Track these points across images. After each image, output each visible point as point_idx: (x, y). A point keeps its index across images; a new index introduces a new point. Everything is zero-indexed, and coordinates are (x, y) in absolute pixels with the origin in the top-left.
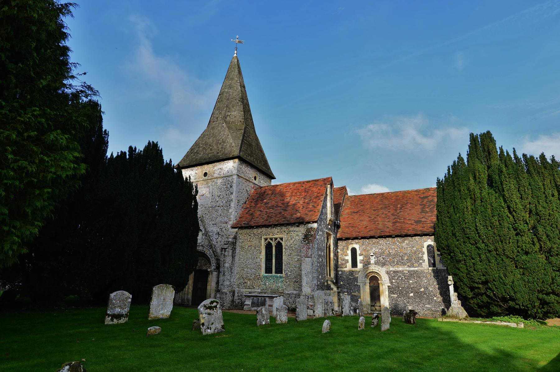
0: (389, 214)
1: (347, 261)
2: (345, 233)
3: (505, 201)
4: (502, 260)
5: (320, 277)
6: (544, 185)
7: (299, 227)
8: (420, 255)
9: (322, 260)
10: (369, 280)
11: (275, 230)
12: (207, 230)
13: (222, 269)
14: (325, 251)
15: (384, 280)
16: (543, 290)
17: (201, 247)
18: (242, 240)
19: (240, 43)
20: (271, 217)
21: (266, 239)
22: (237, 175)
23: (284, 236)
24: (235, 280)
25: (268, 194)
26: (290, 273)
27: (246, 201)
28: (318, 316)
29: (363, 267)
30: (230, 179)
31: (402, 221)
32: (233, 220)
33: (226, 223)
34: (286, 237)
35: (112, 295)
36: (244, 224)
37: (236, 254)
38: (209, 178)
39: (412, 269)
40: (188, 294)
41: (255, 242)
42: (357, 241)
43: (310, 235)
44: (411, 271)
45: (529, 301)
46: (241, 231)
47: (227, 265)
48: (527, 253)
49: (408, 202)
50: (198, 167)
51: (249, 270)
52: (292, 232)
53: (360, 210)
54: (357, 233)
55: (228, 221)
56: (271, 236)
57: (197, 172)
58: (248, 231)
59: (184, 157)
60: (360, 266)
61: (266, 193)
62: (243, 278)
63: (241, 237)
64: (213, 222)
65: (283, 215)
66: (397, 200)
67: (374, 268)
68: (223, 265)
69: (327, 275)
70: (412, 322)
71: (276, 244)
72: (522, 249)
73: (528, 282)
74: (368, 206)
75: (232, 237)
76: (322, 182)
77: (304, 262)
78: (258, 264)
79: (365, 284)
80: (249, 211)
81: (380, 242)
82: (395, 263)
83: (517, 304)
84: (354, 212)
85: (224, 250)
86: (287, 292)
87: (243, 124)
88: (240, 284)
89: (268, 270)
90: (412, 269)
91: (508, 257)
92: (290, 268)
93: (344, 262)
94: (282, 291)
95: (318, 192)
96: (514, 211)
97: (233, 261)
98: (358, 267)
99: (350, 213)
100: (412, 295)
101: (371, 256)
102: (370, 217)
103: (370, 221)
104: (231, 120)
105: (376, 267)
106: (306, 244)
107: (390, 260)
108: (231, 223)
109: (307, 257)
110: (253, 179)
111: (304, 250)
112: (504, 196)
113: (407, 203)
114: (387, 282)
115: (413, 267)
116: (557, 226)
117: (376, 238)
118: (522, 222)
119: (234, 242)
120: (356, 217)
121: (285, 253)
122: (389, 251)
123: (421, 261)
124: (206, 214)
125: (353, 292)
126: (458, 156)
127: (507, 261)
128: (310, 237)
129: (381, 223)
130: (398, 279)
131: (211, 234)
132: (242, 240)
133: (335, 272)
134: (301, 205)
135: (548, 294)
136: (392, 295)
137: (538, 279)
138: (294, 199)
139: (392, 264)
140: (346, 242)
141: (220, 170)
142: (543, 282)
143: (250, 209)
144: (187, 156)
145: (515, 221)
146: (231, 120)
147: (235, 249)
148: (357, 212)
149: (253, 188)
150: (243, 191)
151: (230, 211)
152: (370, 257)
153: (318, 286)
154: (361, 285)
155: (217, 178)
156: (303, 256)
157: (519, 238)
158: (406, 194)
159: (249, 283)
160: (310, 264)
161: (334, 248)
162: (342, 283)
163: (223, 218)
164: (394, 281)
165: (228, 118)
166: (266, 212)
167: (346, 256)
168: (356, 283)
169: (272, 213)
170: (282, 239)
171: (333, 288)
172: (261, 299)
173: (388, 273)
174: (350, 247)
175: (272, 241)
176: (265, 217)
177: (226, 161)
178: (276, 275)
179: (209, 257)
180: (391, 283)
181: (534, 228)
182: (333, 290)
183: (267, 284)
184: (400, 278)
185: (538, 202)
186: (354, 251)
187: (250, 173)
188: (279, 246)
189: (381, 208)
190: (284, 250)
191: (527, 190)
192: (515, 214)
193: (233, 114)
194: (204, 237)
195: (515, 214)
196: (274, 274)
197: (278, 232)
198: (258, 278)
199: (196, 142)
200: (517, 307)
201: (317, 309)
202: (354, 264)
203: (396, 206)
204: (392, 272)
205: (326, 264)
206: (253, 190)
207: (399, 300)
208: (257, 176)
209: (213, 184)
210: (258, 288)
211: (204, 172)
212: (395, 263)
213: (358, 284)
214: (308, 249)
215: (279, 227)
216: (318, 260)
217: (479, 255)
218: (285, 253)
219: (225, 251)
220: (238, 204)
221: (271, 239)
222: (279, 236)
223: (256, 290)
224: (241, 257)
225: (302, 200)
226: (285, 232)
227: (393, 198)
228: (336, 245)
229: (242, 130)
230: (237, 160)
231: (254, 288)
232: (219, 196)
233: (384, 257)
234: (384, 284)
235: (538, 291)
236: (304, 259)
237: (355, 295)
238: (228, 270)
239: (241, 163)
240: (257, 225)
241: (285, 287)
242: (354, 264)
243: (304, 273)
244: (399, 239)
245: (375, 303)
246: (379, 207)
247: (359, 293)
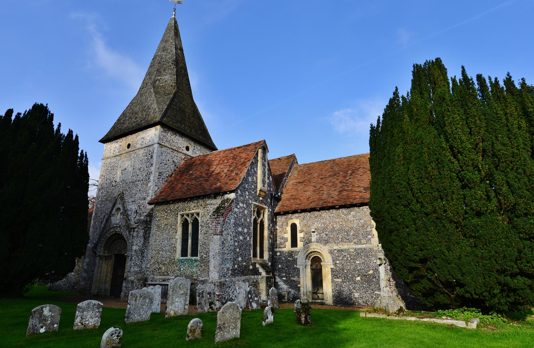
0: (337, 182)
1: (286, 240)
2: (284, 206)
3: (447, 140)
4: (444, 226)
5: (240, 259)
6: (506, 114)
7: (216, 199)
8: (369, 229)
9: (245, 239)
10: (311, 262)
11: (192, 204)
12: (126, 209)
13: (130, 253)
14: (252, 228)
15: (326, 261)
16: (506, 270)
17: (118, 228)
18: (159, 218)
20: (190, 190)
21: (182, 216)
22: (158, 143)
23: (200, 211)
24: (148, 266)
25: (196, 165)
26: (205, 256)
27: (172, 174)
28: (175, 313)
29: (304, 246)
30: (151, 149)
31: (350, 188)
32: (151, 195)
33: (145, 199)
37: (151, 235)
39: (359, 246)
40: (105, 283)
41: (171, 220)
42: (297, 215)
43: (222, 207)
44: (359, 249)
45: (486, 287)
46: (158, 208)
48: (479, 214)
49: (361, 166)
50: (122, 138)
51: (164, 253)
52: (209, 206)
53: (306, 180)
54: (297, 206)
55: (146, 196)
56: (187, 212)
57: (121, 144)
58: (165, 207)
59: (111, 129)
60: (300, 244)
61: (194, 164)
62: (158, 262)
63: (157, 215)
64: (133, 199)
66: (348, 165)
67: (315, 247)
68: (131, 248)
69: (255, 255)
70: (303, 322)
71: (193, 220)
72: (471, 209)
73: (483, 258)
74: (316, 175)
75: (145, 214)
76: (254, 146)
77: (212, 241)
78: (173, 246)
79: (306, 267)
80: (172, 184)
81: (323, 215)
82: (340, 240)
83: (467, 292)
84: (299, 183)
85: (132, 230)
86: (201, 279)
87: (174, 89)
88: (155, 269)
89: (184, 253)
90: (359, 246)
91: (451, 221)
92: (206, 249)
93: (283, 241)
94: (196, 278)
95: (246, 157)
96: (459, 152)
97: (144, 244)
98: (298, 246)
99: (295, 184)
100: (358, 278)
101: (313, 232)
102: (315, 187)
103: (314, 191)
104: (161, 85)
105: (318, 246)
106: (216, 218)
107: (334, 236)
108: (149, 199)
109: (216, 235)
110: (184, 149)
111: (213, 226)
112: (445, 133)
113: (359, 168)
114: (330, 264)
115: (361, 244)
116: (525, 172)
117: (319, 211)
118: (471, 168)
119: (148, 220)
120: (300, 187)
121: (201, 231)
122: (332, 226)
123: (370, 237)
124: (126, 190)
125: (292, 277)
126: (394, 90)
127: (451, 227)
128: (222, 210)
129: (325, 193)
130: (342, 259)
131: (129, 213)
132: (159, 218)
133: (271, 253)
135: (513, 276)
136: (336, 280)
137: (496, 253)
138: (219, 167)
139: (336, 242)
140: (285, 217)
141: (142, 140)
142: (505, 257)
143: (174, 182)
144: (113, 128)
145: (461, 167)
146: (161, 85)
147: (150, 228)
148: (302, 182)
149: (184, 159)
150: (168, 162)
151: (149, 185)
152: (312, 233)
153: (233, 270)
154: (301, 268)
155: (139, 149)
156: (212, 233)
157: (467, 192)
158: (360, 158)
159: (163, 268)
160: (219, 243)
161: (269, 225)
162: (280, 266)
163: (142, 193)
164: (338, 262)
165: (157, 83)
167: (285, 233)
168: (295, 266)
171: (261, 273)
172: (165, 288)
173: (331, 252)
174: (290, 223)
175: (189, 217)
177: (148, 129)
178: (191, 258)
179: (126, 239)
180: (335, 264)
181: (490, 176)
182: (261, 275)
183: (182, 269)
184: (345, 259)
185: (496, 137)
186: (294, 227)
187: (181, 142)
188: (196, 223)
189: (330, 176)
190: (200, 228)
191: (478, 122)
192: (460, 157)
193: (164, 78)
194: (122, 216)
195: (460, 157)
196: (189, 257)
197: (194, 207)
198: (173, 262)
199: (124, 112)
200: (468, 295)
201: (172, 303)
202: (294, 243)
203: (346, 172)
204: (336, 251)
205: (252, 243)
206: (183, 161)
207: (344, 285)
209: (135, 155)
210: (172, 274)
211: (127, 143)
212: (340, 240)
213: (298, 267)
214: (217, 224)
215: (196, 200)
216: (237, 237)
217: (414, 220)
218: (201, 231)
219: (134, 231)
220: (160, 176)
221: (188, 215)
222: (196, 211)
224: (157, 238)
226: (201, 205)
227: (345, 164)
228: (273, 222)
229: (171, 94)
230: (158, 127)
232: (140, 169)
233: (327, 233)
234: (326, 266)
235: (498, 271)
236: (213, 237)
237: (294, 281)
238: (137, 254)
239: (165, 130)
240: (173, 199)
241: (199, 273)
242: (294, 243)
243: (211, 254)
244: (344, 211)
245: (318, 290)
246: (328, 175)
247: (299, 277)
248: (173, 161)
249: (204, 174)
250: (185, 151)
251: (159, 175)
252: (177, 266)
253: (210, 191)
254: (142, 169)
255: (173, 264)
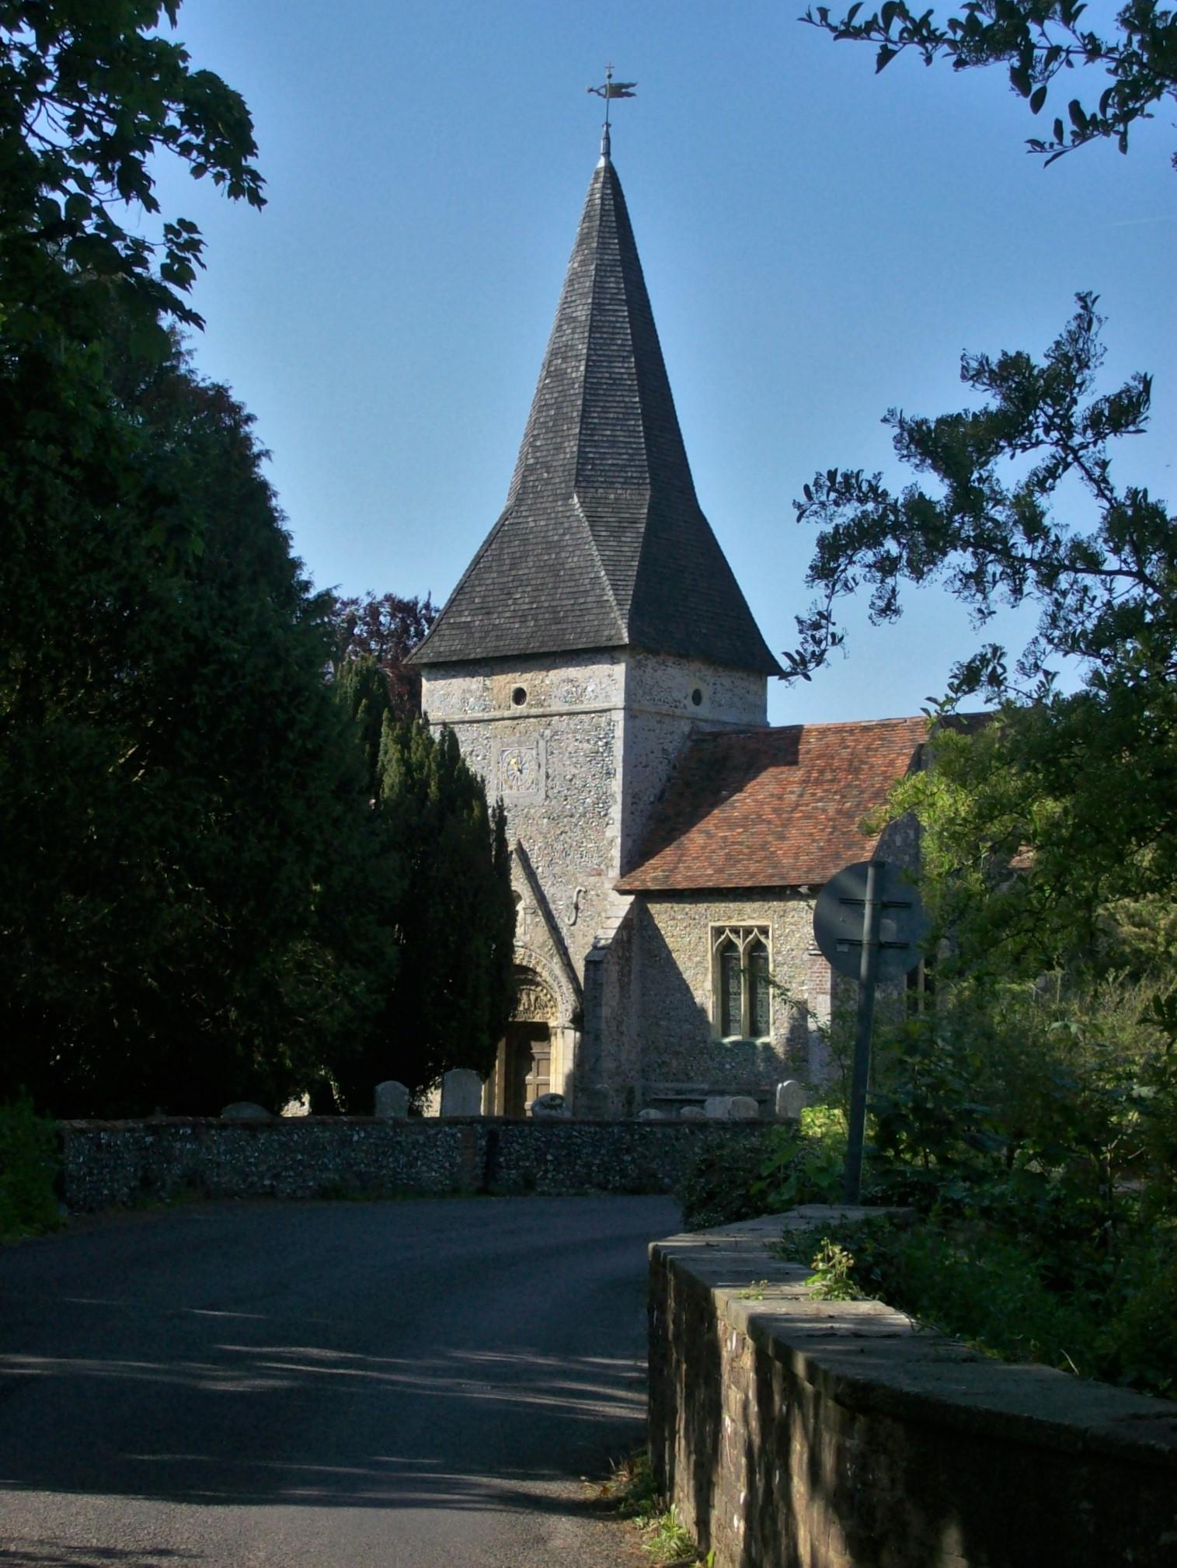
11: (748, 907)
19: (622, 95)
27: (663, 792)
33: (600, 875)
34: (776, 926)
35: (380, 1088)
36: (655, 879)
38: (534, 711)
47: (605, 1012)
56: (734, 923)
65: (772, 853)
94: (767, 1088)
95: (886, 772)
110: (689, 702)
134: (830, 820)
138: (814, 794)
141: (568, 687)
155: (561, 715)
159: (674, 1063)
166: (722, 837)
169: (741, 843)
170: (764, 931)
176: (719, 858)
183: (728, 1066)
208: (702, 687)
221: (735, 930)
223: (695, 1086)
225: (834, 800)
231: (690, 1079)
248: (663, 749)
249: (767, 809)
250: (692, 708)
251: (633, 804)
252: (713, 1060)
253: (794, 874)
254: (578, 783)
255: (702, 1053)
